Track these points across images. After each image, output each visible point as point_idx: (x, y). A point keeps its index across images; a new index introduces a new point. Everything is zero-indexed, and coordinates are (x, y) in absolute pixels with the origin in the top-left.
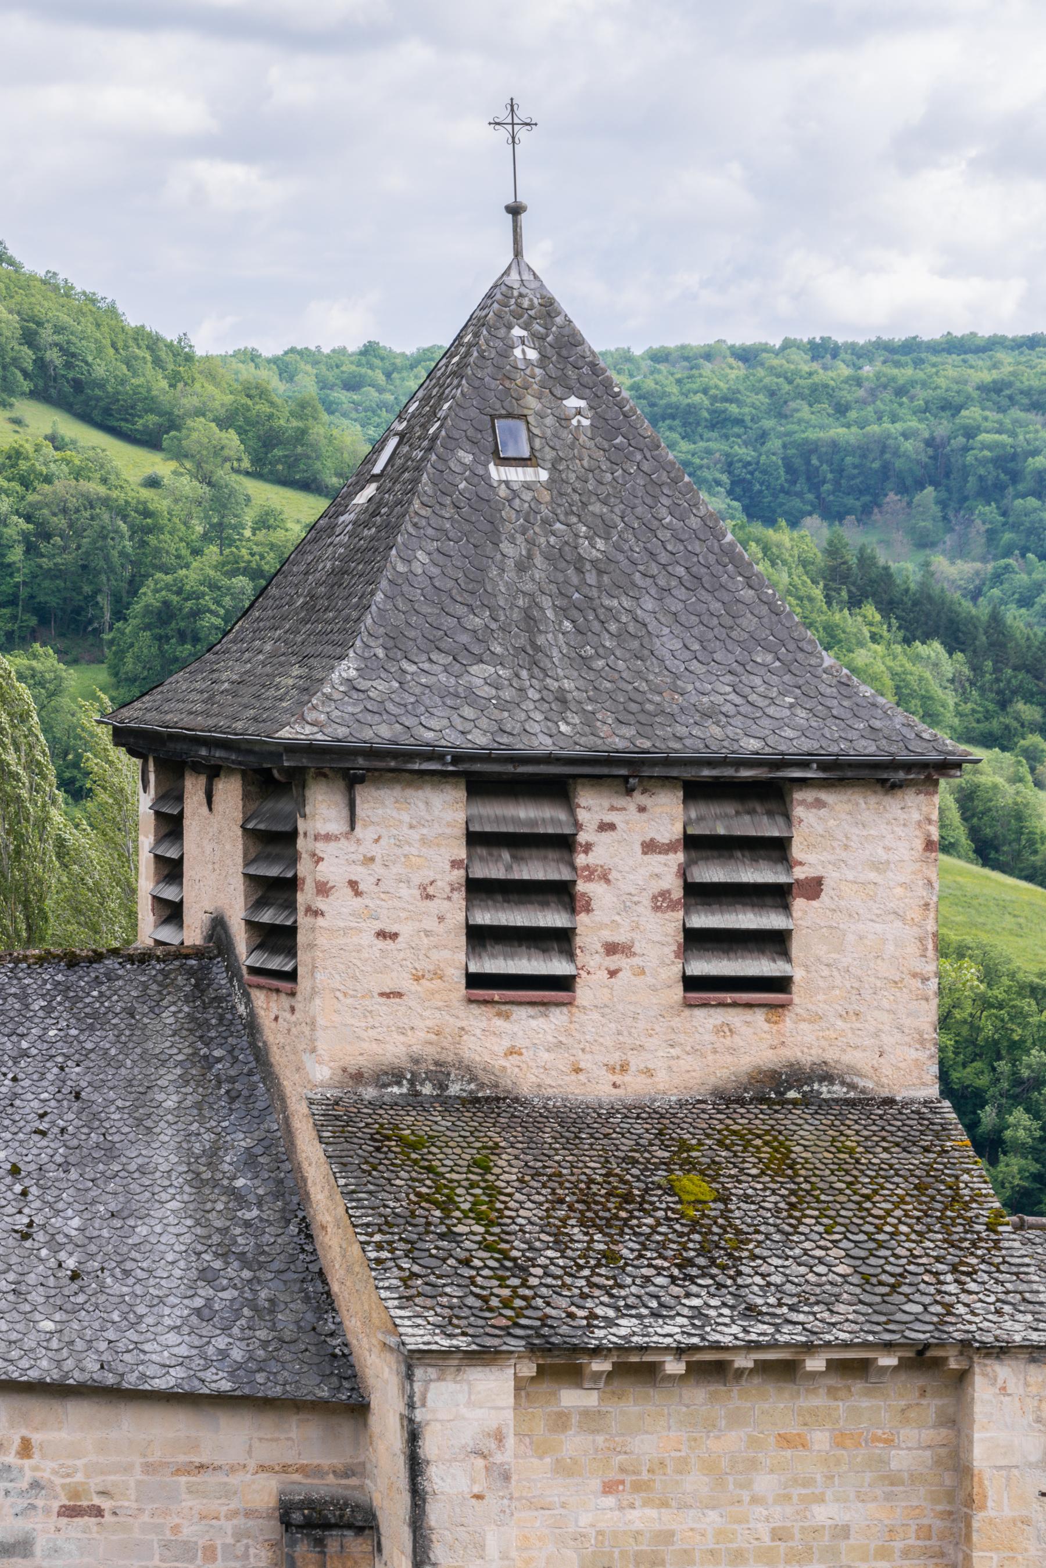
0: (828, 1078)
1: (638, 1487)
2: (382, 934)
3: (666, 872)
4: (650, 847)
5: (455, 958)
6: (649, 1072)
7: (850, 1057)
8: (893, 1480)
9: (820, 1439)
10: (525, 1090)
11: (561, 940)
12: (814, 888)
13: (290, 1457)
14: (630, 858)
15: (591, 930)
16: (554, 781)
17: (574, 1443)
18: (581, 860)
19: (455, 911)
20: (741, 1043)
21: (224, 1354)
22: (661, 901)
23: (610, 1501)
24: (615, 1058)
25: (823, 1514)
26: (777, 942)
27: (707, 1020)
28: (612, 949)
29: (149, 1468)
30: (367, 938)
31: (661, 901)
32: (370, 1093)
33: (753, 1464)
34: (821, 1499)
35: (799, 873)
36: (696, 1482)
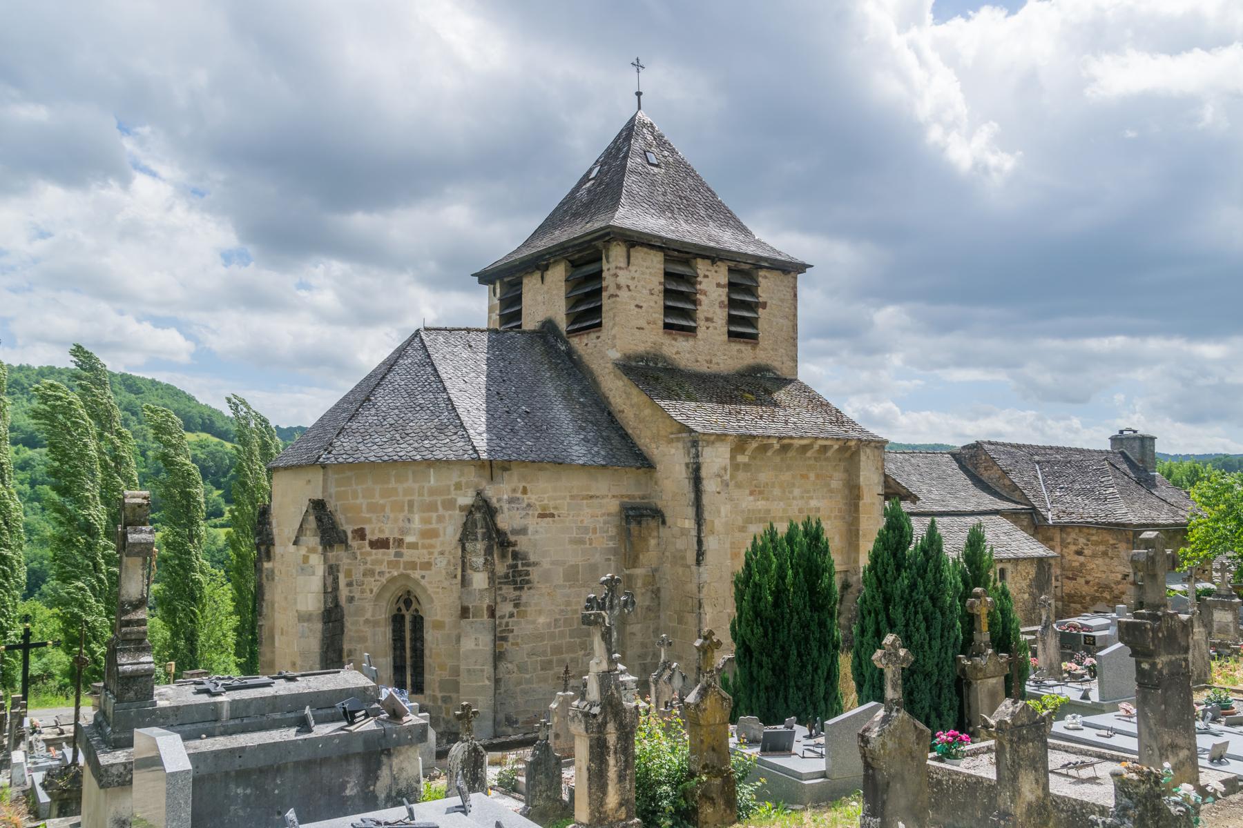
0: (768, 370)
1: (761, 493)
2: (637, 306)
4: (718, 285)
5: (659, 317)
6: (718, 364)
7: (776, 364)
8: (831, 491)
9: (812, 476)
10: (681, 367)
12: (764, 305)
13: (624, 492)
14: (712, 287)
15: (702, 312)
18: (698, 287)
21: (598, 453)
23: (751, 498)
24: (708, 358)
27: (735, 347)
28: (707, 319)
29: (572, 497)
30: (633, 307)
32: (634, 364)
33: (794, 485)
34: (812, 498)
35: (761, 300)
36: (777, 492)
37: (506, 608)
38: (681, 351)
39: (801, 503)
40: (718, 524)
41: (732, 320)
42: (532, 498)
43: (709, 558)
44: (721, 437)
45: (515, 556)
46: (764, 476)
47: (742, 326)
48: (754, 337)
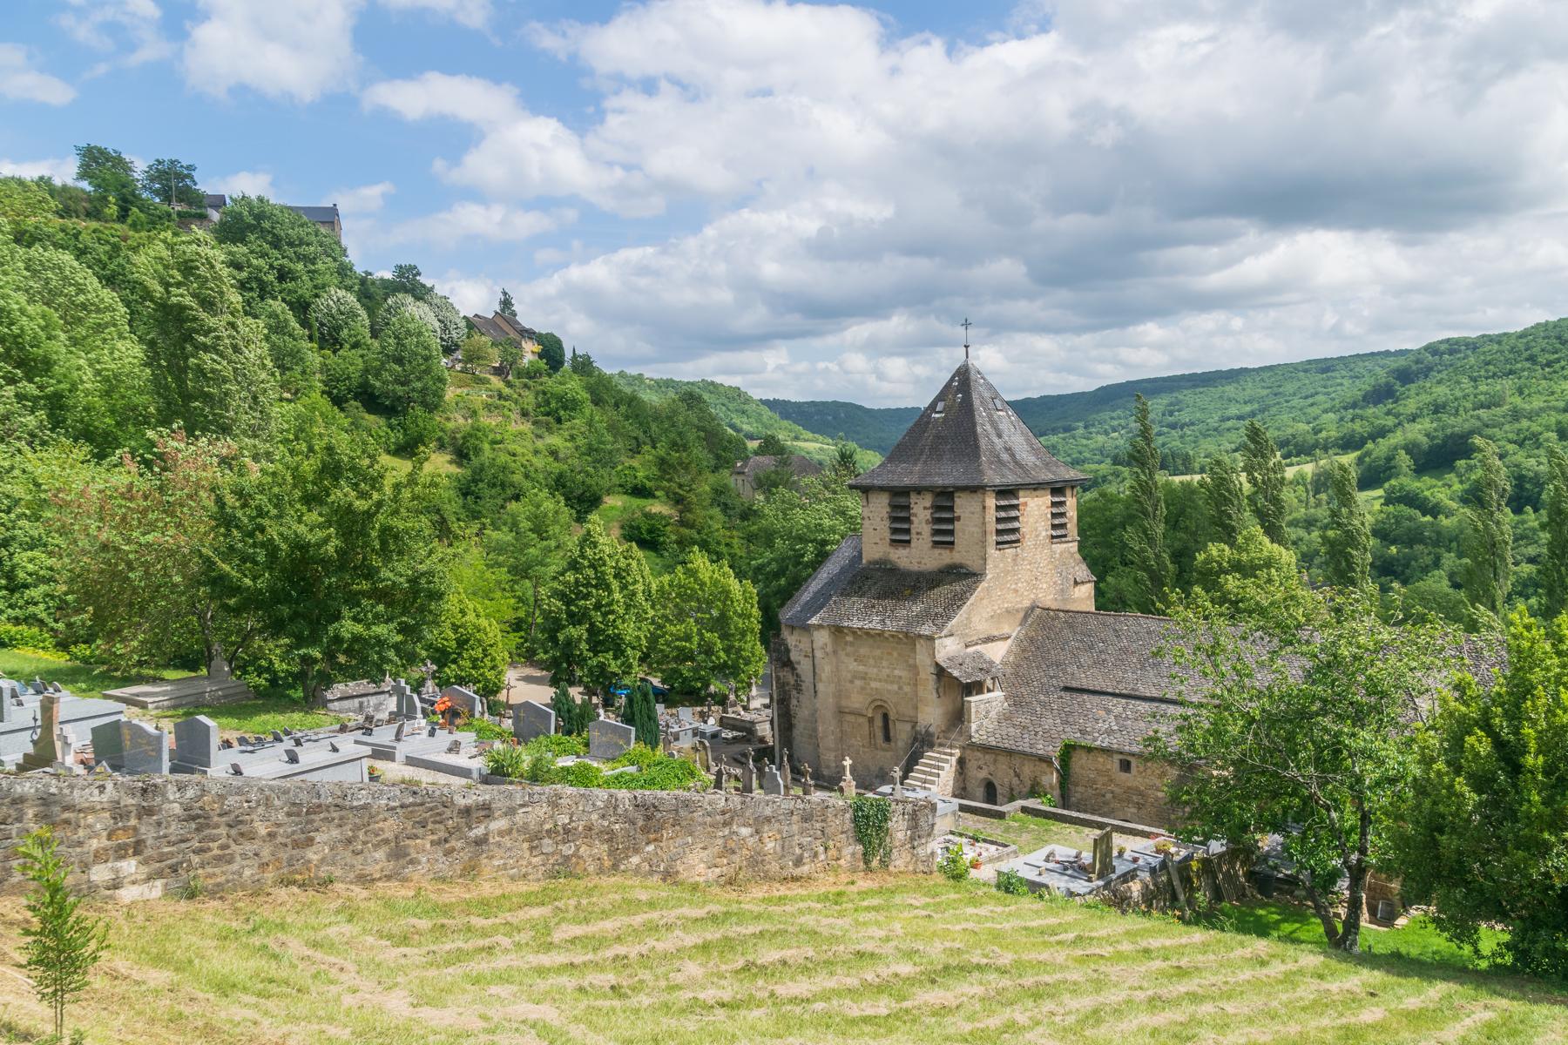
3: (927, 514)
5: (888, 535)
11: (908, 531)
12: (959, 519)
14: (921, 510)
15: (914, 528)
16: (904, 492)
17: (849, 649)
19: (887, 523)
20: (943, 558)
22: (927, 522)
25: (897, 672)
26: (951, 532)
27: (937, 551)
31: (927, 522)
36: (871, 661)
38: (904, 559)
40: (824, 676)
41: (936, 532)
42: (801, 646)
44: (820, 627)
46: (862, 651)
47: (944, 536)
48: (952, 543)
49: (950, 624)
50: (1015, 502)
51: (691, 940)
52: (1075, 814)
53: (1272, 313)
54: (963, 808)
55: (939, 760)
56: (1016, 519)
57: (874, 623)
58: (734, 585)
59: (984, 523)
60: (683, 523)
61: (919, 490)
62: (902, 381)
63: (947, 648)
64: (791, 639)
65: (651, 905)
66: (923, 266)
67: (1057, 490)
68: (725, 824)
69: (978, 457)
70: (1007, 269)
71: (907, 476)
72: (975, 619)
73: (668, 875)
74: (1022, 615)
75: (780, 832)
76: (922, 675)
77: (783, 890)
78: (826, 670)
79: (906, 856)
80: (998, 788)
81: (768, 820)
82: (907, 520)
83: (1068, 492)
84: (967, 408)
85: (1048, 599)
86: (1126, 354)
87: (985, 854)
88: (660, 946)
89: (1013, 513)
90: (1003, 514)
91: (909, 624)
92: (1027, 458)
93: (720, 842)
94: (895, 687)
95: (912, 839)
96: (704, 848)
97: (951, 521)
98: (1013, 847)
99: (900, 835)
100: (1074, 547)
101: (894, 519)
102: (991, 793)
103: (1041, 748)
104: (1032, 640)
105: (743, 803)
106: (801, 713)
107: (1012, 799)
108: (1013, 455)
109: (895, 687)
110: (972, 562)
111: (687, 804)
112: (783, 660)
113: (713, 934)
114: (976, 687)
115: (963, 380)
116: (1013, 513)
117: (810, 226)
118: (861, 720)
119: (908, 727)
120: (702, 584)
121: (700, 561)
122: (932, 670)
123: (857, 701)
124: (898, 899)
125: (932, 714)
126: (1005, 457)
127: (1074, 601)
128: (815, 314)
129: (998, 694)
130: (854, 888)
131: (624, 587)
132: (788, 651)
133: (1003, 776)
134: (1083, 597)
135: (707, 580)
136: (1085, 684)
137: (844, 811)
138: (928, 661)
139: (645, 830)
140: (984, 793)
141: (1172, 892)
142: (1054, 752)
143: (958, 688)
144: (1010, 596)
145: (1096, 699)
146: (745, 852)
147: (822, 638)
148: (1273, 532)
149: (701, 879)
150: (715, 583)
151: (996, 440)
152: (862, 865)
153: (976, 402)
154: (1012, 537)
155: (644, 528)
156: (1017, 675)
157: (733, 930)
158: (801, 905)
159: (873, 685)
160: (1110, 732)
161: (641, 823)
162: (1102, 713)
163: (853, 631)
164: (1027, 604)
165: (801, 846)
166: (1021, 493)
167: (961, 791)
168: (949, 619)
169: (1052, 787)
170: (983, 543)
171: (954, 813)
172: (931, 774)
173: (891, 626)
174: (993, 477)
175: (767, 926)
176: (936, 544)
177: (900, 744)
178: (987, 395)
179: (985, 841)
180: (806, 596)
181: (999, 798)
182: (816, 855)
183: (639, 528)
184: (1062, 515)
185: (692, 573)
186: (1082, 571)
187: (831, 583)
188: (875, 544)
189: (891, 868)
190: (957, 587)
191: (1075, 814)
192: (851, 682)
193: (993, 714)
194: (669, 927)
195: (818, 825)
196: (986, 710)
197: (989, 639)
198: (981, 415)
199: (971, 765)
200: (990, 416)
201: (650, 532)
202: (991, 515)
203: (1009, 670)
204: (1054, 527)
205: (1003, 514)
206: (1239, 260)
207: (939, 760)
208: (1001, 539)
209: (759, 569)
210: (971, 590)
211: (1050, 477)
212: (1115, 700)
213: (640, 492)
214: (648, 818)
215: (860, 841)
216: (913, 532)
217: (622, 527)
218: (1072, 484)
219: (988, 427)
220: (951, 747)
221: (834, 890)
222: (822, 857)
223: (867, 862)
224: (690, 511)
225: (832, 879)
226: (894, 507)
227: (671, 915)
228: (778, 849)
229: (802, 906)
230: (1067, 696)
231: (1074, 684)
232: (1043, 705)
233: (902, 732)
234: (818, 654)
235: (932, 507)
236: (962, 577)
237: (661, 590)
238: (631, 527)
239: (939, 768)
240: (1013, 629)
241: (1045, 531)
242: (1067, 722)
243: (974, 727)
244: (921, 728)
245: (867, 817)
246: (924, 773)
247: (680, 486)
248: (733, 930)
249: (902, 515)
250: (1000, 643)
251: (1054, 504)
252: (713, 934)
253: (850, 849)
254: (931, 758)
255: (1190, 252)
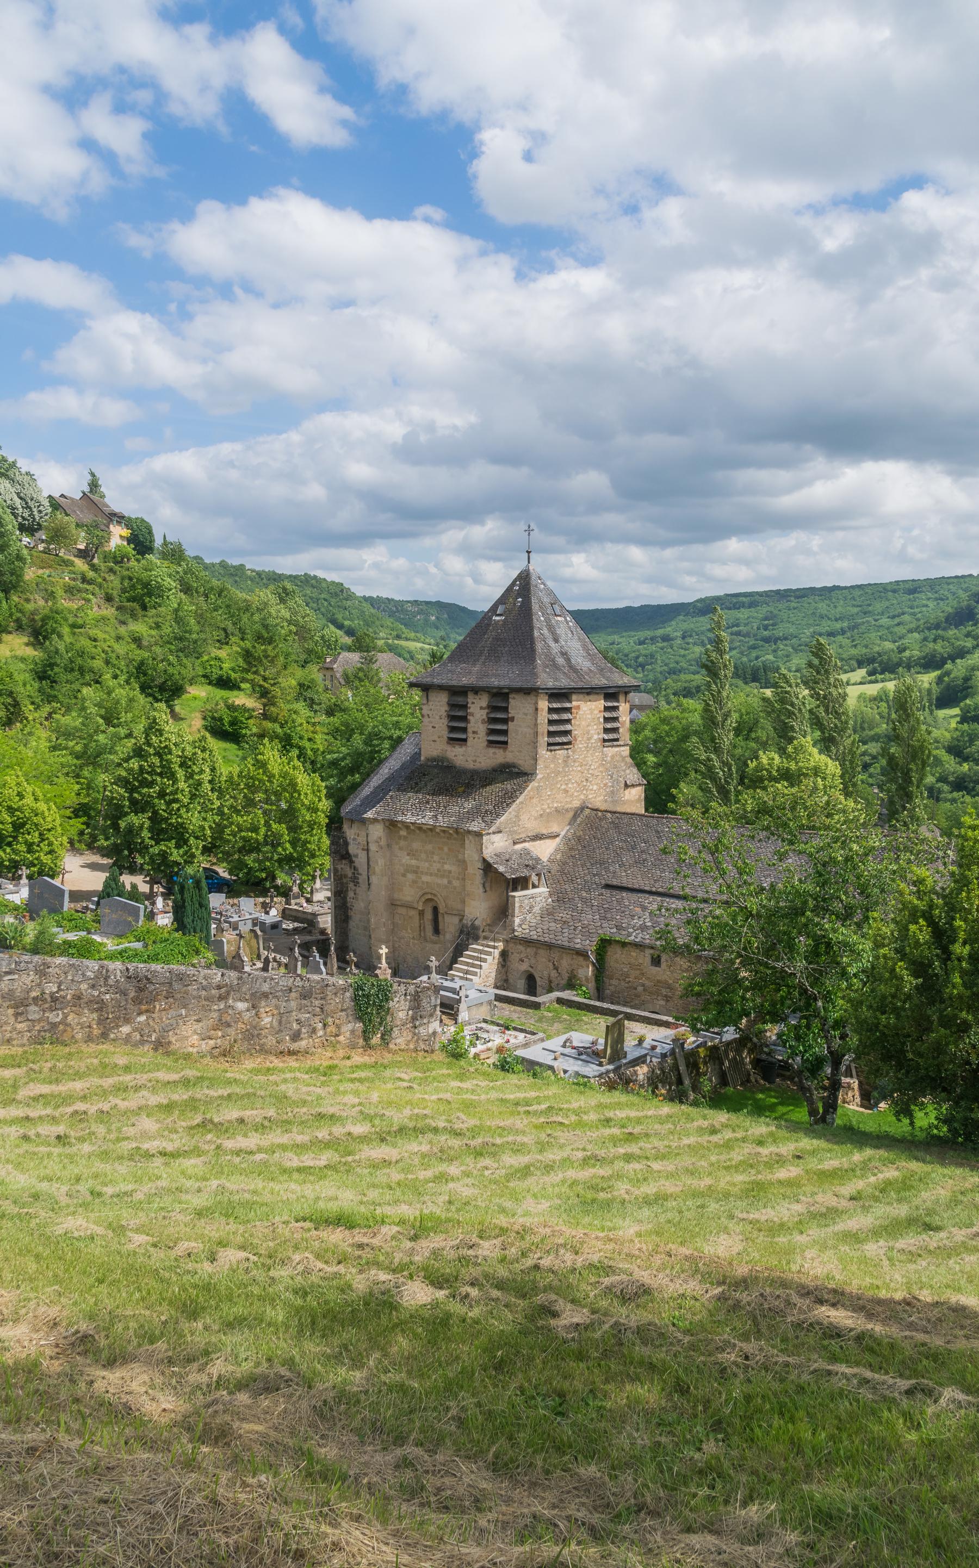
4: (481, 708)
5: (445, 733)
7: (520, 762)
9: (446, 849)
11: (464, 730)
12: (513, 719)
15: (471, 727)
17: (402, 843)
22: (483, 722)
25: (447, 867)
26: (505, 733)
27: (491, 750)
28: (474, 732)
31: (483, 722)
36: (423, 856)
37: (351, 894)
39: (438, 866)
41: (491, 732)
43: (372, 887)
45: (355, 868)
46: (416, 845)
47: (498, 736)
49: (498, 821)
50: (568, 705)
51: (154, 1100)
52: (605, 1005)
53: (840, 534)
54: (499, 998)
55: (481, 952)
56: (568, 721)
57: (426, 819)
58: (303, 779)
59: (536, 725)
60: (265, 716)
61: (476, 690)
62: (480, 584)
63: (495, 845)
64: (350, 832)
65: (127, 1069)
66: (518, 476)
67: (612, 694)
68: (221, 998)
69: (533, 659)
70: (592, 481)
71: (465, 676)
72: (524, 817)
73: (159, 1045)
74: (571, 814)
75: (277, 1007)
76: (470, 870)
77: (277, 1062)
78: (380, 864)
79: (407, 1035)
80: (538, 979)
81: (265, 996)
82: (464, 719)
83: (622, 698)
84: (526, 612)
85: (598, 800)
86: (718, 571)
87: (512, 1041)
88: (122, 1105)
89: (565, 716)
90: (555, 717)
91: (460, 819)
92: (581, 661)
93: (215, 1015)
94: (445, 881)
95: (414, 1019)
96: (198, 1021)
97: (505, 721)
98: (541, 1035)
99: (402, 1015)
100: (626, 751)
101: (452, 718)
102: (531, 985)
103: (579, 942)
104: (579, 839)
105: (240, 978)
106: (357, 906)
107: (550, 990)
108: (568, 660)
109: (445, 881)
110: (524, 763)
111: (181, 977)
112: (341, 852)
113: (180, 1095)
114: (521, 883)
115: (523, 586)
116: (565, 716)
117: (395, 431)
118: (413, 913)
119: (456, 920)
120: (271, 777)
121: (271, 753)
122: (480, 865)
123: (409, 894)
124: (388, 1073)
125: (478, 908)
126: (560, 661)
127: (624, 803)
128: (405, 518)
129: (543, 890)
130: (348, 1063)
131: (189, 776)
132: (346, 844)
133: (543, 971)
134: (633, 799)
135: (276, 772)
136: (625, 882)
137: (345, 990)
138: (476, 857)
139: (137, 1001)
140: (523, 986)
141: (679, 1078)
142: (590, 946)
143: (504, 883)
144: (560, 796)
145: (634, 897)
146: (240, 1025)
147: (377, 831)
148: (827, 743)
149: (195, 1050)
150: (284, 775)
151: (552, 644)
152: (361, 1042)
153: (535, 607)
154: (564, 739)
155: (226, 720)
156: (562, 872)
157: (201, 1092)
158: (288, 1076)
159: (426, 878)
160: (643, 928)
161: (132, 994)
162: (638, 910)
163: (407, 826)
164: (576, 804)
165: (298, 1021)
166: (574, 697)
167: (503, 981)
168: (498, 816)
169: (587, 979)
170: (534, 744)
171: (490, 1003)
172: (473, 966)
173: (442, 822)
174: (546, 680)
175: (238, 1090)
176: (491, 743)
177: (448, 936)
178: (546, 600)
179: (515, 1029)
180: (366, 791)
181: (539, 990)
182: (314, 1031)
183: (221, 719)
184: (615, 719)
185: (262, 765)
186: (633, 775)
187: (391, 779)
188: (432, 740)
189: (391, 1046)
190: (508, 786)
191: (605, 1005)
192: (404, 875)
193: (537, 909)
194: (137, 1088)
195: (317, 1003)
196: (531, 904)
197: (538, 837)
198: (539, 619)
199: (514, 958)
200: (548, 621)
201: (232, 723)
202: (543, 717)
203: (555, 868)
204: (606, 731)
205: (555, 717)
206: (809, 482)
207: (481, 952)
208: (552, 740)
209: (334, 763)
210: (521, 789)
211: (603, 682)
212: (651, 898)
213: (224, 683)
214: (141, 990)
215: (360, 1019)
216: (470, 730)
217: (204, 718)
218: (626, 690)
219: (545, 631)
220: (494, 940)
221: (326, 1063)
222: (321, 1033)
223: (366, 1039)
224: (274, 704)
225: (329, 1054)
226: (452, 706)
227: (142, 1078)
228: (275, 1024)
229: (293, 1079)
230: (607, 893)
231: (615, 882)
232: (585, 901)
233: (450, 925)
234: (373, 847)
235: (489, 707)
236: (513, 775)
237: (230, 780)
238: (213, 718)
239: (481, 960)
240: (562, 828)
241: (596, 733)
242: (605, 918)
243: (517, 921)
244: (468, 921)
245: (368, 996)
246: (467, 964)
247: (265, 679)
248: (201, 1092)
249: (460, 714)
250: (548, 841)
251: (607, 709)
252: (180, 1095)
253: (350, 1026)
254: (475, 950)
255: (764, 476)
